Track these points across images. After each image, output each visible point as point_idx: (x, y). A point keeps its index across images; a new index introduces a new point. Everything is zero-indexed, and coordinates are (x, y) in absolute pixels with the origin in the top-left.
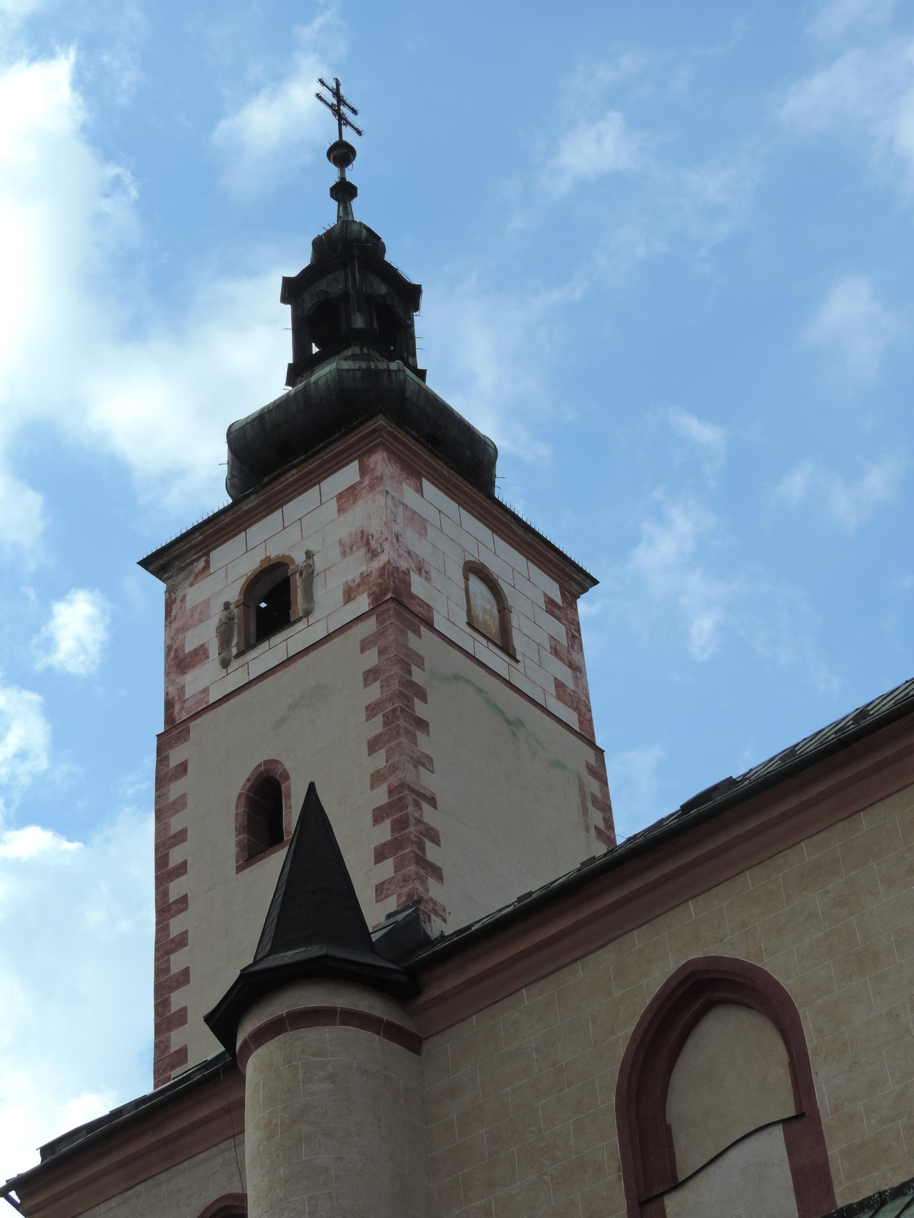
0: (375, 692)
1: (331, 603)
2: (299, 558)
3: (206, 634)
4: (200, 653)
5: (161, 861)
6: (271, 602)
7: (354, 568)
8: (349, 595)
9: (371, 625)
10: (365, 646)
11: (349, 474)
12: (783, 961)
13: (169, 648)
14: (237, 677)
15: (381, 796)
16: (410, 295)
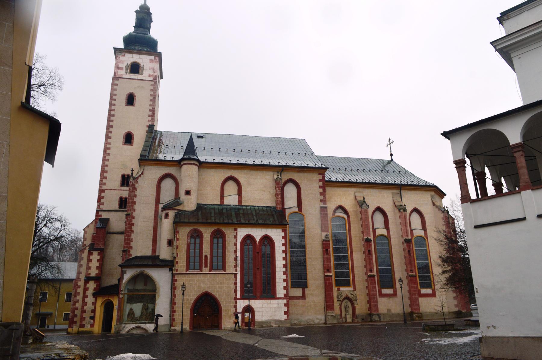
0: (152, 93)
1: (146, 74)
2: (142, 65)
3: (123, 66)
4: (121, 68)
5: (111, 97)
6: (135, 68)
7: (151, 73)
8: (150, 76)
9: (153, 83)
10: (151, 85)
11: (152, 57)
12: (242, 180)
13: (116, 64)
14: (128, 76)
15: (151, 108)
16: (152, 21)
